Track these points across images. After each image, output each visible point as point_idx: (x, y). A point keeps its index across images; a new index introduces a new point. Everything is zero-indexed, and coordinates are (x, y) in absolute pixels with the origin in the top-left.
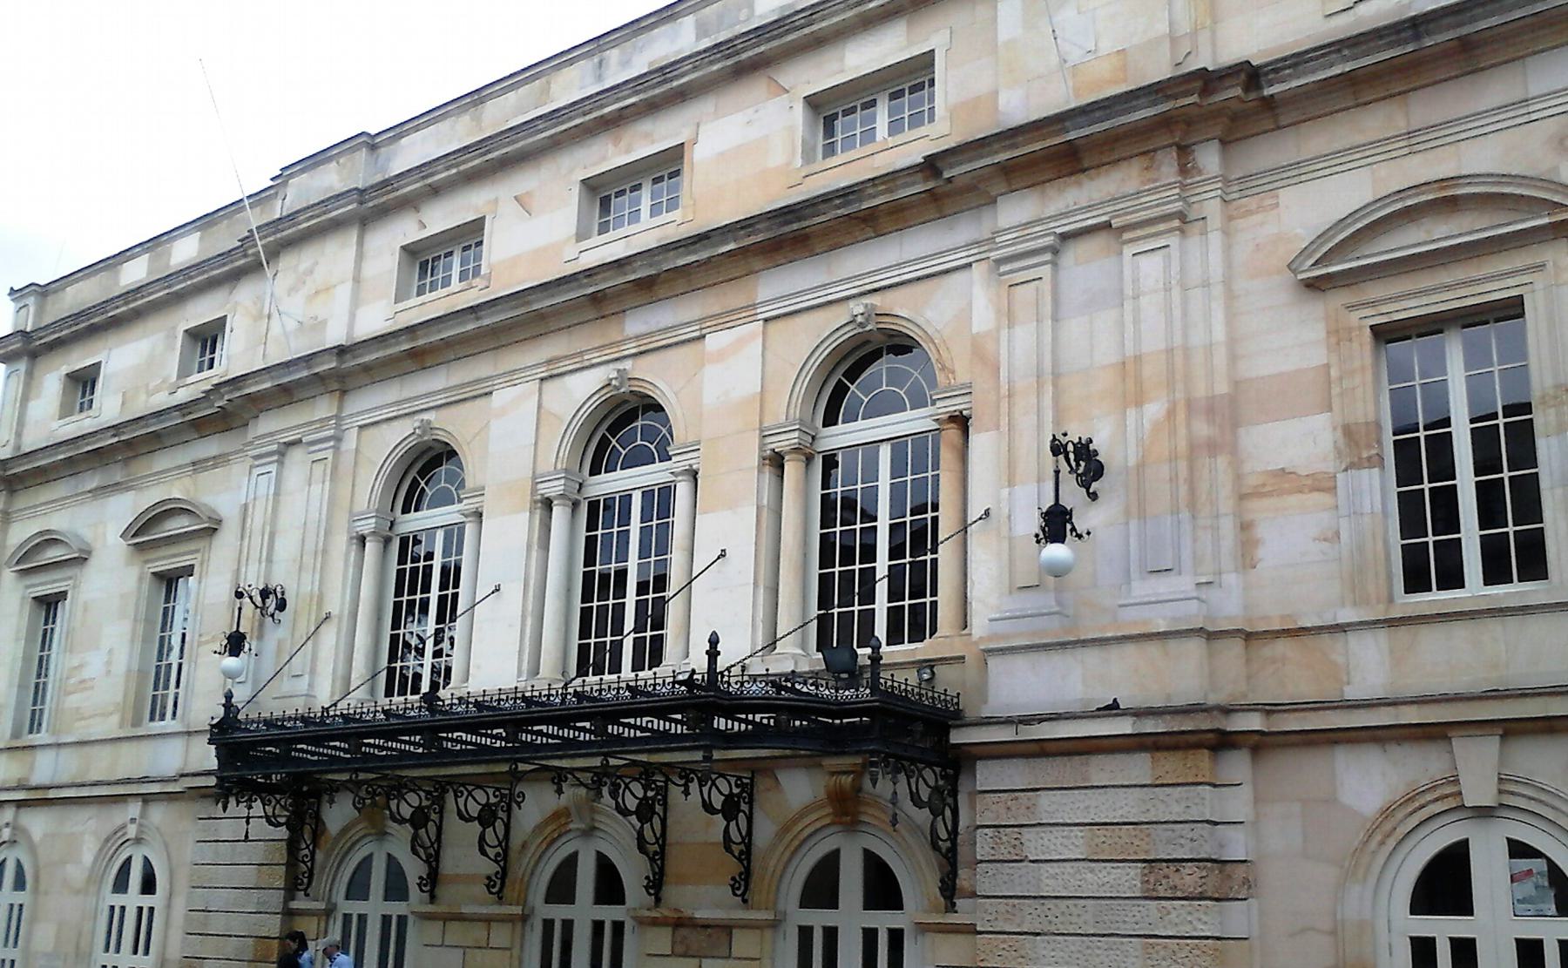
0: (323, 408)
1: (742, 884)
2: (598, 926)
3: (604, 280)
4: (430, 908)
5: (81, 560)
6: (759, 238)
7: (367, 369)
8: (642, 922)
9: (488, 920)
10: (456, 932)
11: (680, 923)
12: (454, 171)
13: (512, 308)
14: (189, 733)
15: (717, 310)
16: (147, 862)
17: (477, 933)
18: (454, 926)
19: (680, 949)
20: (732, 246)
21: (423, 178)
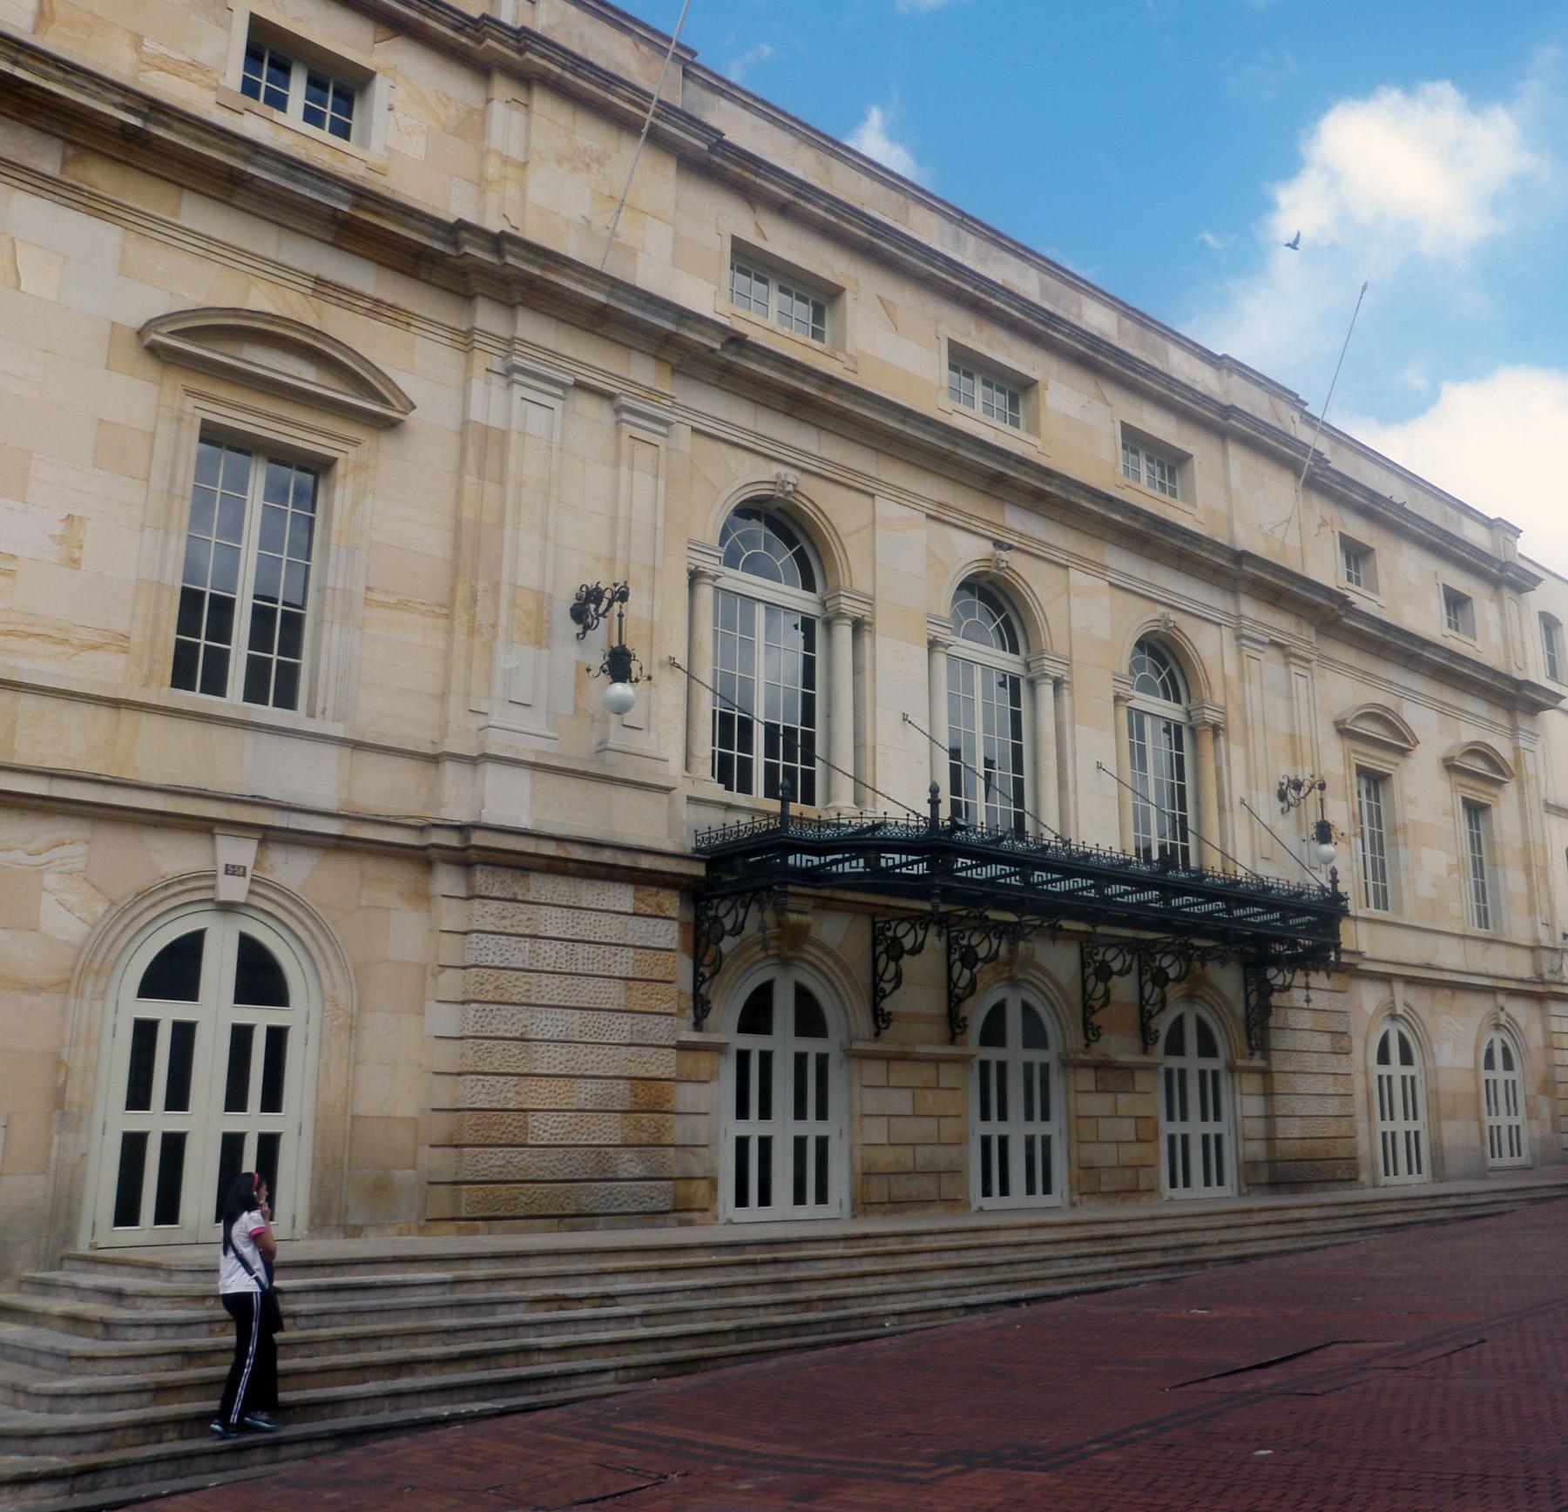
0: (642, 371)
1: (1146, 1036)
2: (1028, 1067)
3: (1025, 474)
4: (694, 1037)
5: (387, 425)
6: (1137, 526)
7: (842, 416)
8: (852, 1055)
9: (936, 1060)
10: (902, 1073)
11: (1103, 1067)
12: (833, 219)
13: (940, 438)
14: (357, 745)
15: (1076, 550)
16: (1027, 1008)
17: (926, 1074)
18: (896, 1066)
19: (1101, 1087)
20: (1118, 518)
21: (796, 194)
